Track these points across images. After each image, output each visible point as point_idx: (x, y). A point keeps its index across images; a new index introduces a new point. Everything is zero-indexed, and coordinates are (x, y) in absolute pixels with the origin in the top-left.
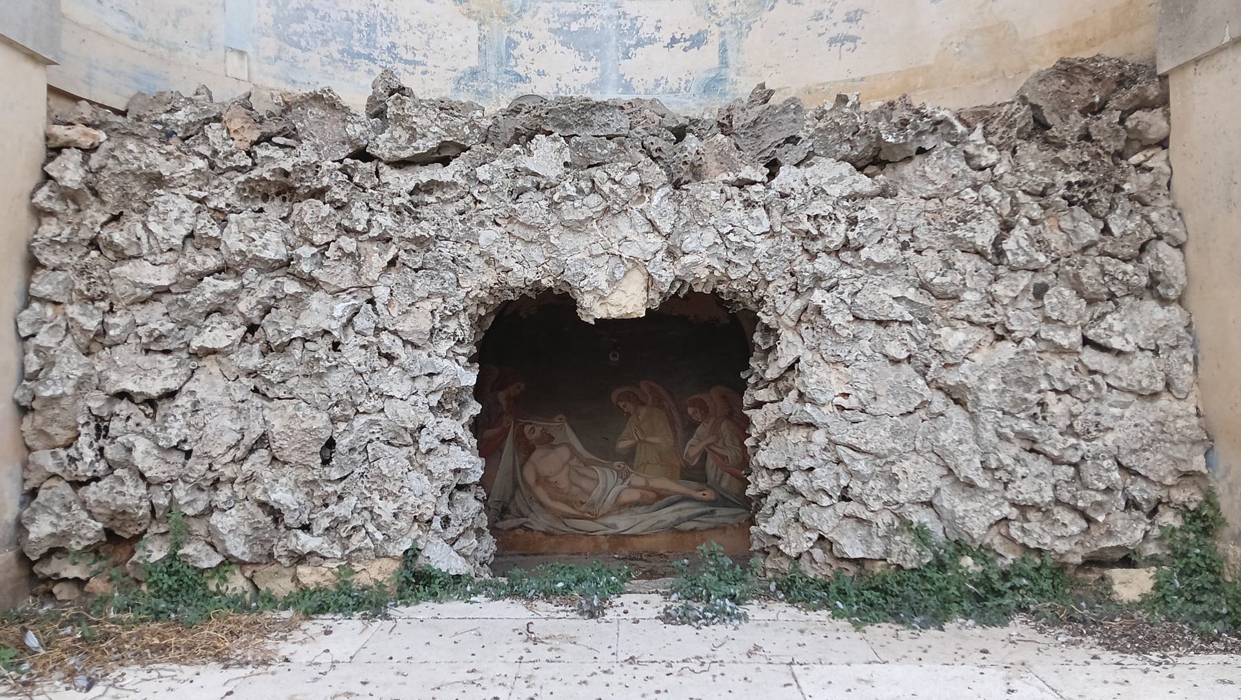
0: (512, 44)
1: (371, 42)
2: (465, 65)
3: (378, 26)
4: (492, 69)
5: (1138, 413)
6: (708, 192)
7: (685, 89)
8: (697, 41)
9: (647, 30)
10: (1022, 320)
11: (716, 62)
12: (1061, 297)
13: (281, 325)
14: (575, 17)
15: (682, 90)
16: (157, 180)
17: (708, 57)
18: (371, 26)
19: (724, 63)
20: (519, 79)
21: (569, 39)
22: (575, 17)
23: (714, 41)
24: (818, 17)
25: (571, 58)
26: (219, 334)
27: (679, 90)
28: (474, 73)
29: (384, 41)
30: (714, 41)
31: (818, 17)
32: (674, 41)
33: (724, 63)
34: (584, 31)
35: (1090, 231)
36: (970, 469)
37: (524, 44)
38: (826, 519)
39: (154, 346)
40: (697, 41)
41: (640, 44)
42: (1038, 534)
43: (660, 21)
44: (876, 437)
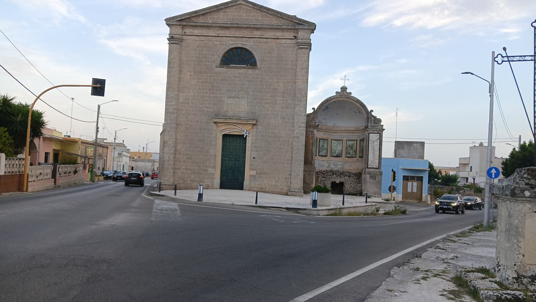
5: (359, 188)
6: (342, 178)
8: (341, 165)
10: (355, 184)
12: (356, 183)
13: (324, 183)
16: (319, 177)
17: (342, 166)
26: (322, 183)
28: (328, 167)
35: (358, 181)
36: (352, 190)
38: (346, 192)
39: (319, 183)
40: (341, 165)
42: (354, 193)
44: (348, 188)
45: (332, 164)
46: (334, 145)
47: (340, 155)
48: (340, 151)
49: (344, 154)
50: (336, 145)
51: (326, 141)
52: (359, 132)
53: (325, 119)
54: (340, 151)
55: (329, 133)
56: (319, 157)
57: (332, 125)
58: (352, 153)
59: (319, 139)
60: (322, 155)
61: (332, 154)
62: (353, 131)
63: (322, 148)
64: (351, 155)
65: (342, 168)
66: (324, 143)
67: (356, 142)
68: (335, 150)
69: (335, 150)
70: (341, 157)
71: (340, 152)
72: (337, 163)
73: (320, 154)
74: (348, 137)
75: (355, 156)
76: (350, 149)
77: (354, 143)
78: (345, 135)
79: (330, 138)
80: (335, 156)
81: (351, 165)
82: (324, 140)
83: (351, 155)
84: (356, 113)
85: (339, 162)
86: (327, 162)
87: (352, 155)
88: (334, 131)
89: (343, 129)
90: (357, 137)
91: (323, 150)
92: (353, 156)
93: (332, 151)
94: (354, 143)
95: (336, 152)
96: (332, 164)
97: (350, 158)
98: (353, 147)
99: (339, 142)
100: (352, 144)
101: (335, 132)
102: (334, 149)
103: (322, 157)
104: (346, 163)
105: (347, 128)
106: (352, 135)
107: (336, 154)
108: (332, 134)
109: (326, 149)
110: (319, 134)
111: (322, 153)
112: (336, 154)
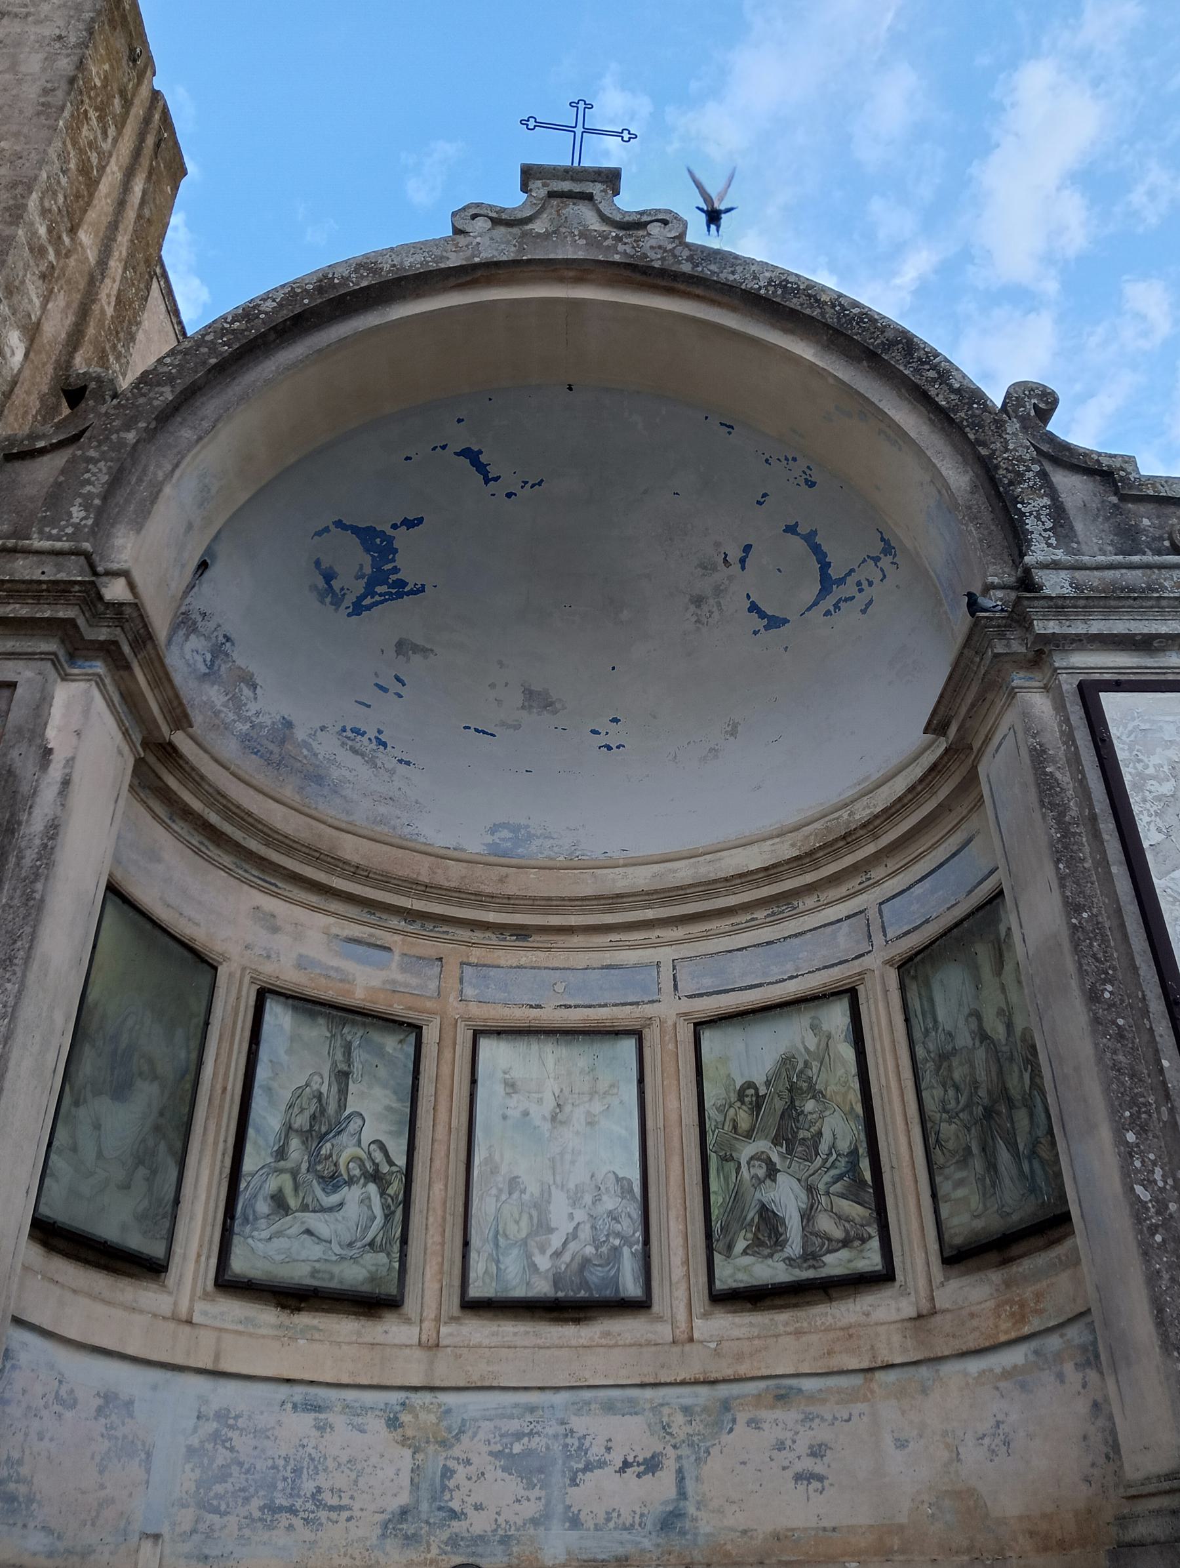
0: (447, 1473)
1: (294, 1492)
2: (394, 1504)
3: (305, 1470)
4: (424, 1506)
7: (640, 1525)
8: (652, 1465)
9: (596, 1451)
11: (672, 1493)
14: (518, 1436)
15: (637, 1526)
17: (663, 1486)
18: (297, 1471)
19: (682, 1494)
20: (454, 1515)
21: (510, 1462)
22: (518, 1436)
23: (670, 1464)
24: (780, 1446)
25: (512, 1486)
27: (632, 1525)
28: (404, 1513)
29: (308, 1486)
30: (670, 1464)
31: (780, 1446)
32: (626, 1465)
33: (682, 1494)
34: (528, 1453)
37: (461, 1472)
40: (652, 1465)
41: (588, 1468)
43: (610, 1440)
45: (481, 1460)
46: (516, 1104)
47: (615, 1281)
48: (610, 1203)
49: (677, 1242)
50: (540, 1112)
51: (393, 1045)
52: (870, 849)
53: (363, 743)
54: (610, 1203)
55: (428, 948)
56: (234, 1310)
57: (475, 845)
58: (807, 1216)
59: (263, 995)
60: (298, 1274)
61: (478, 1265)
62: (770, 872)
63: (296, 1149)
64: (794, 1247)
65: (671, 1521)
66: (342, 1077)
67: (837, 1017)
68: (533, 1189)
69: (533, 1189)
70: (640, 1305)
71: (614, 1216)
72: (579, 1424)
73: (239, 1265)
74: (708, 983)
75: (870, 1259)
76: (762, 1145)
77: (812, 1042)
78: (665, 955)
79: (454, 1007)
80: (542, 1288)
81: (817, 1451)
82: (353, 1034)
83: (794, 1247)
84: (775, 622)
85: (609, 1408)
86: (393, 1423)
87: (810, 1257)
88: (509, 902)
89: (641, 878)
90: (845, 941)
91: (332, 1181)
92: (836, 1263)
93: (484, 1207)
94: (812, 1042)
95: (543, 1227)
96: (476, 1448)
97: (780, 1319)
98: (810, 1105)
99: (579, 1056)
100: (787, 1061)
101: (522, 932)
102: (513, 1183)
103: (304, 1319)
104: (726, 1405)
105: (684, 873)
106: (766, 934)
107: (543, 1262)
108: (476, 955)
109: (376, 1177)
110: (271, 924)
111: (315, 1251)
112: (543, 1262)
